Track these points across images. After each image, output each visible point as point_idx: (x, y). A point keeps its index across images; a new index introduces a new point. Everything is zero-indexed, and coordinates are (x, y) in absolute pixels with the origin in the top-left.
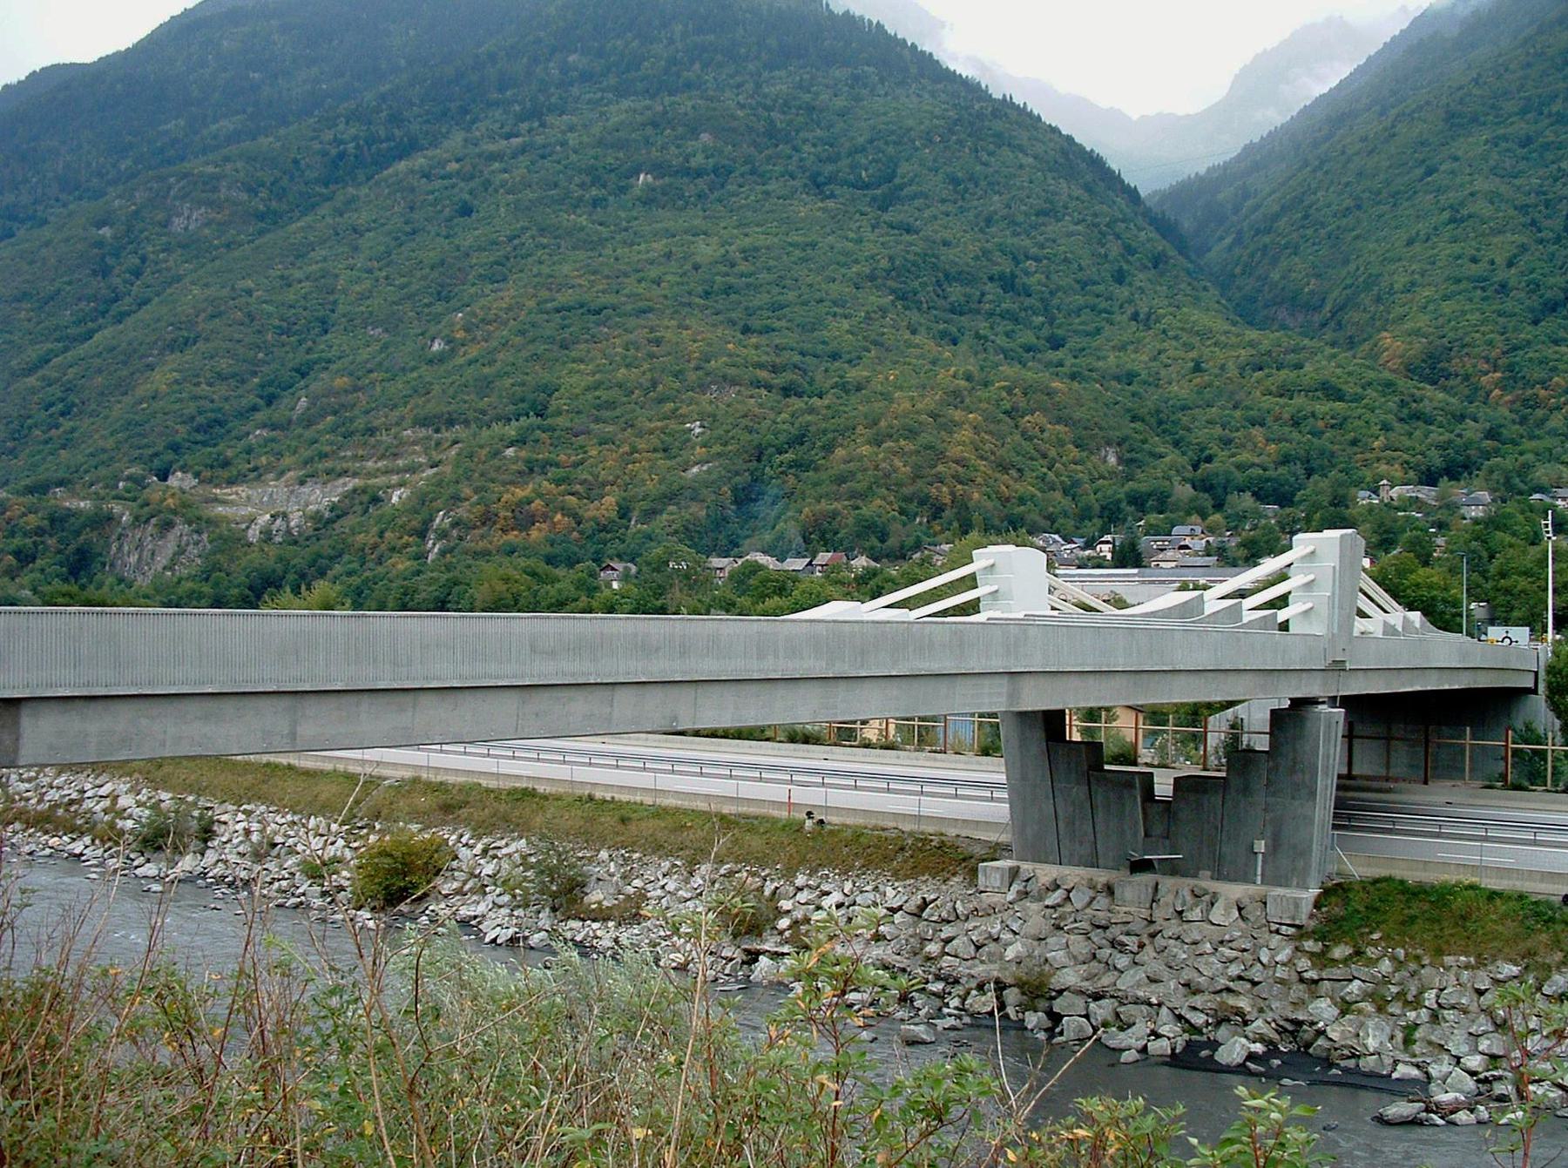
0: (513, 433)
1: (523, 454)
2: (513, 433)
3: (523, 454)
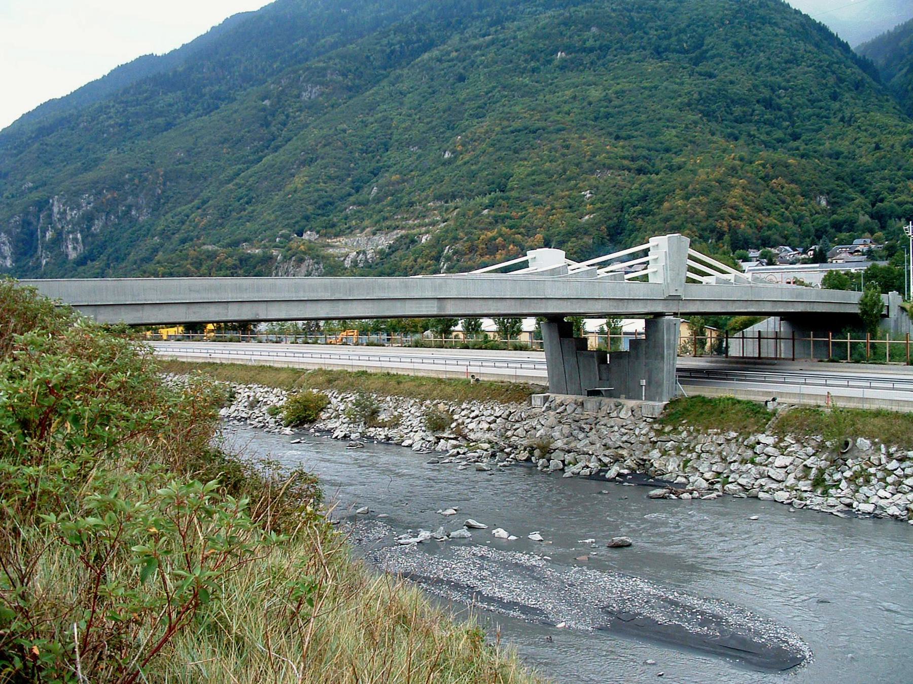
1: (492, 213)
3: (492, 213)
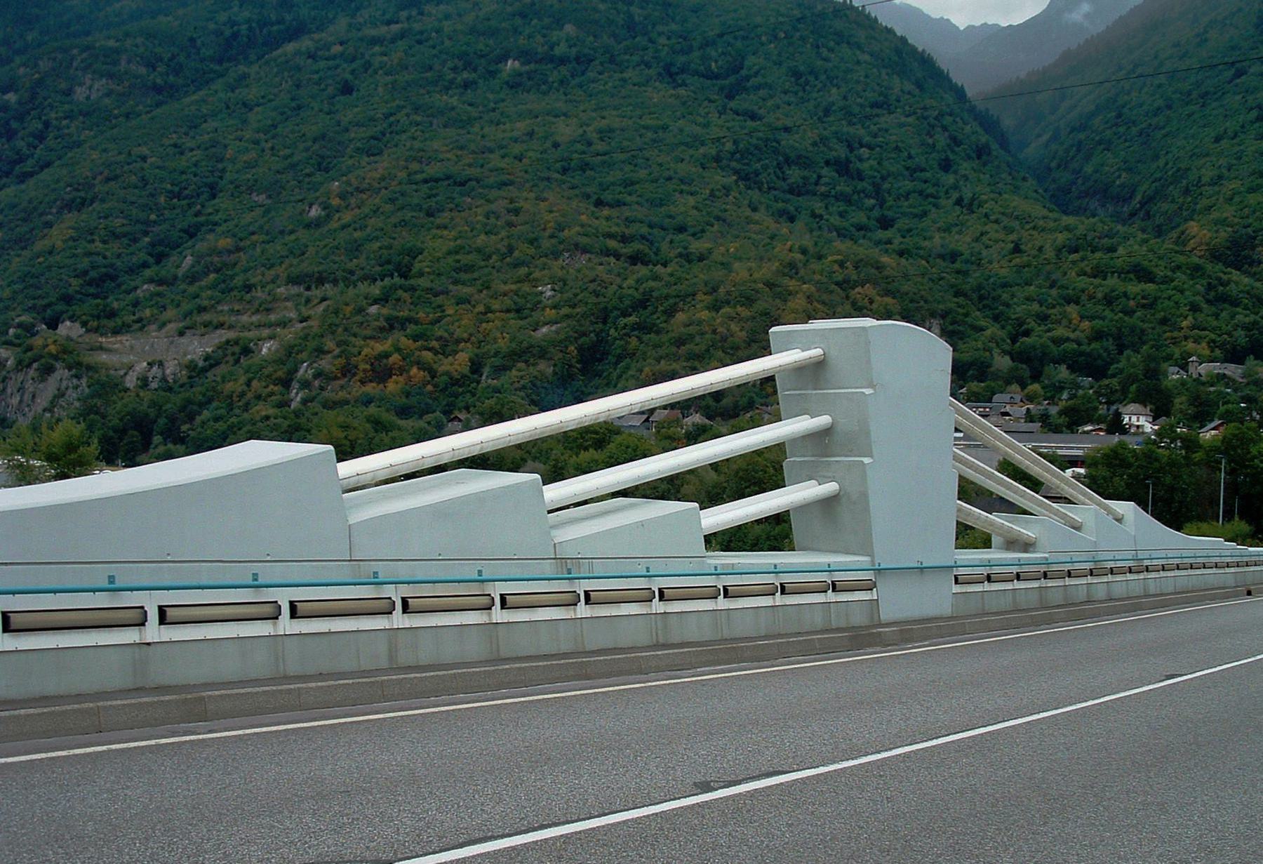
0: (378, 292)
1: (385, 311)
2: (378, 292)
3: (385, 311)
